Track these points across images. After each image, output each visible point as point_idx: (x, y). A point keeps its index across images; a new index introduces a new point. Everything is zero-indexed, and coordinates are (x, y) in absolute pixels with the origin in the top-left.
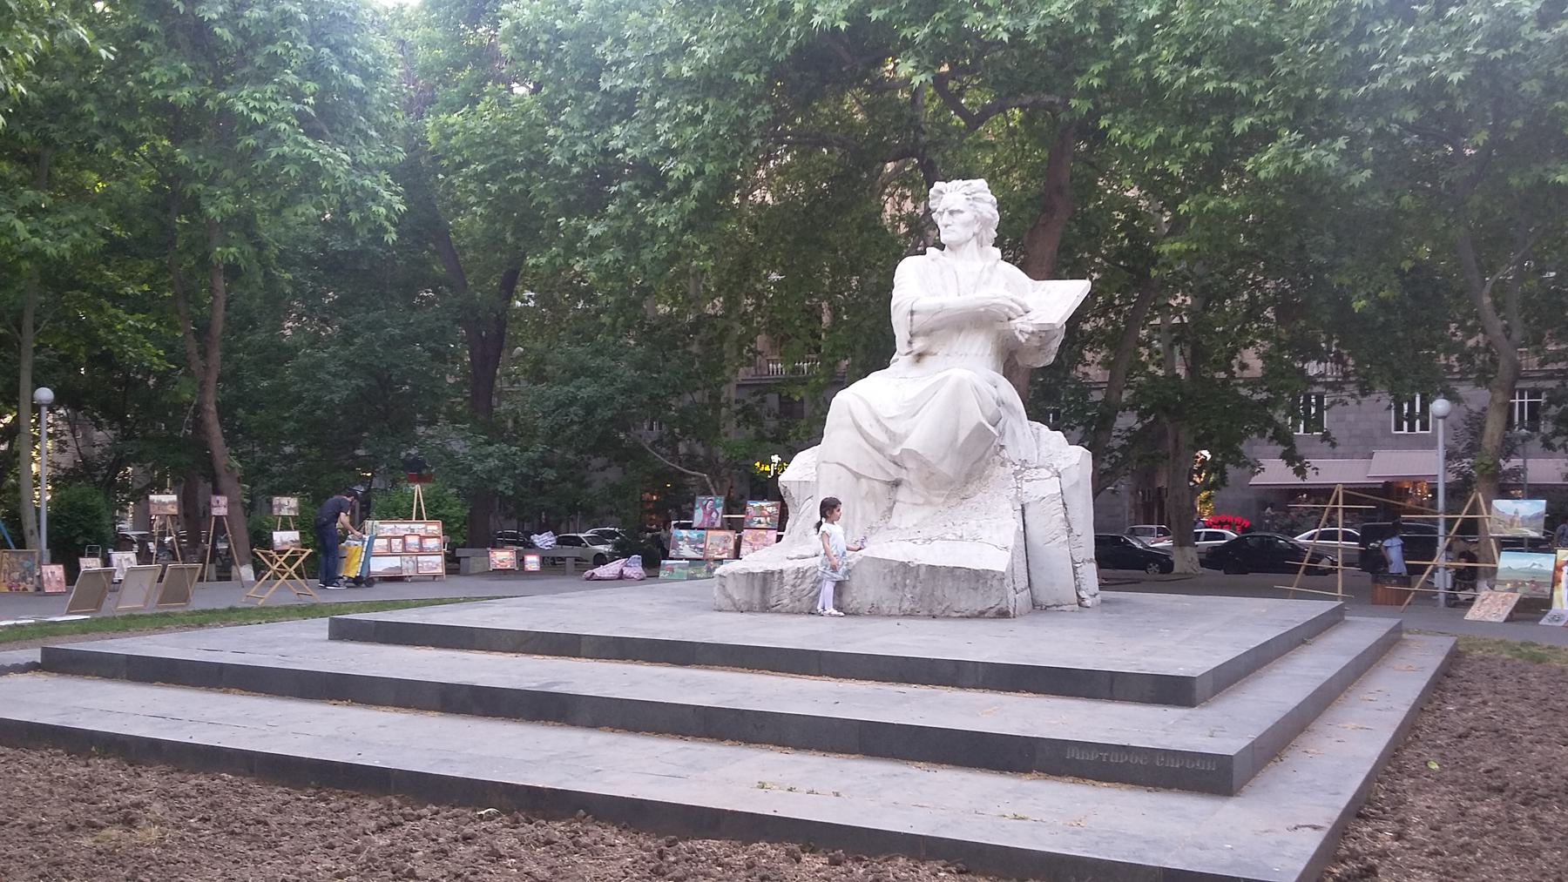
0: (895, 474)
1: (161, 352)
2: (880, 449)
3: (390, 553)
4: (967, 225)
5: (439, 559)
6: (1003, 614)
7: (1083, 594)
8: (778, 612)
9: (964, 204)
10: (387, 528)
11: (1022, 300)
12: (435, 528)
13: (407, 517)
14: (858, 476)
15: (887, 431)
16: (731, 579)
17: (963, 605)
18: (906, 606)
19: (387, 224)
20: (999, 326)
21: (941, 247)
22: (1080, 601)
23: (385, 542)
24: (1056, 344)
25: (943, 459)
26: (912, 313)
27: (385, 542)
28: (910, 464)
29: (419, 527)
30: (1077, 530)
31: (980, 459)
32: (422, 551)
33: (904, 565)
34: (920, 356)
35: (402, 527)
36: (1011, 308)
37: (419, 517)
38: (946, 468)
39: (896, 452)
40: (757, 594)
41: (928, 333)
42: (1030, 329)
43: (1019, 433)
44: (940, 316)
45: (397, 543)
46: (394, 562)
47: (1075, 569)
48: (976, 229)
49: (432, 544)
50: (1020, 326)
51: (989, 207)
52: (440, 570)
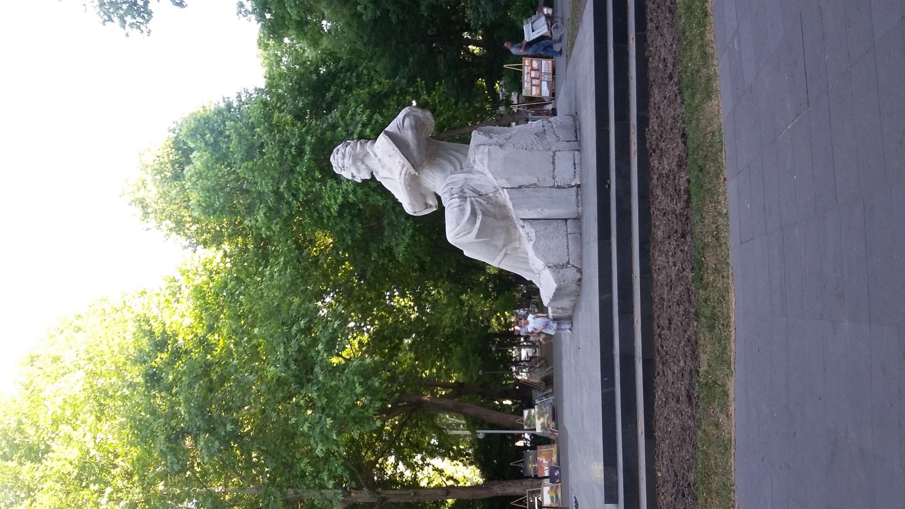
1: (437, 83)
3: (539, 86)
4: (359, 171)
5: (544, 62)
6: (580, 280)
7: (573, 184)
10: (526, 85)
11: (400, 168)
12: (527, 62)
13: (521, 73)
14: (506, 254)
19: (373, 121)
21: (372, 173)
22: (579, 186)
23: (534, 88)
24: (420, 113)
25: (495, 246)
27: (534, 88)
29: (526, 70)
30: (535, 181)
31: (494, 216)
32: (538, 70)
35: (526, 78)
36: (405, 175)
37: (521, 67)
38: (500, 243)
41: (424, 197)
43: (478, 182)
44: (415, 203)
45: (534, 82)
46: (544, 84)
47: (559, 187)
48: (360, 164)
49: (535, 64)
51: (346, 160)
52: (550, 62)
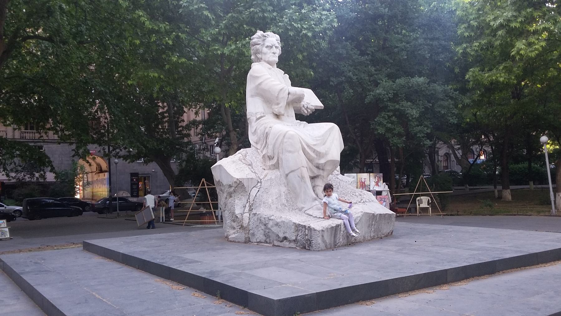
0: (316, 172)
2: (310, 160)
8: (339, 246)
9: (268, 43)
15: (314, 151)
16: (326, 231)
17: (385, 231)
18: (372, 234)
20: (295, 105)
26: (289, 93)
28: (328, 168)
33: (373, 214)
34: (277, 116)
39: (322, 161)
40: (333, 239)
42: (313, 108)
50: (306, 106)
